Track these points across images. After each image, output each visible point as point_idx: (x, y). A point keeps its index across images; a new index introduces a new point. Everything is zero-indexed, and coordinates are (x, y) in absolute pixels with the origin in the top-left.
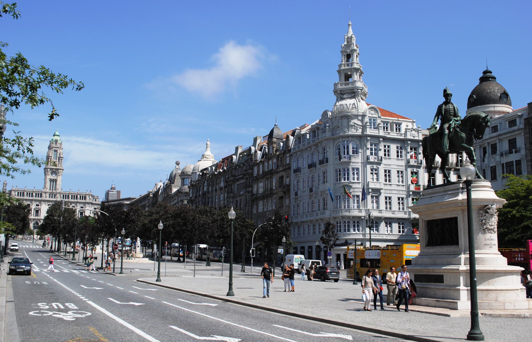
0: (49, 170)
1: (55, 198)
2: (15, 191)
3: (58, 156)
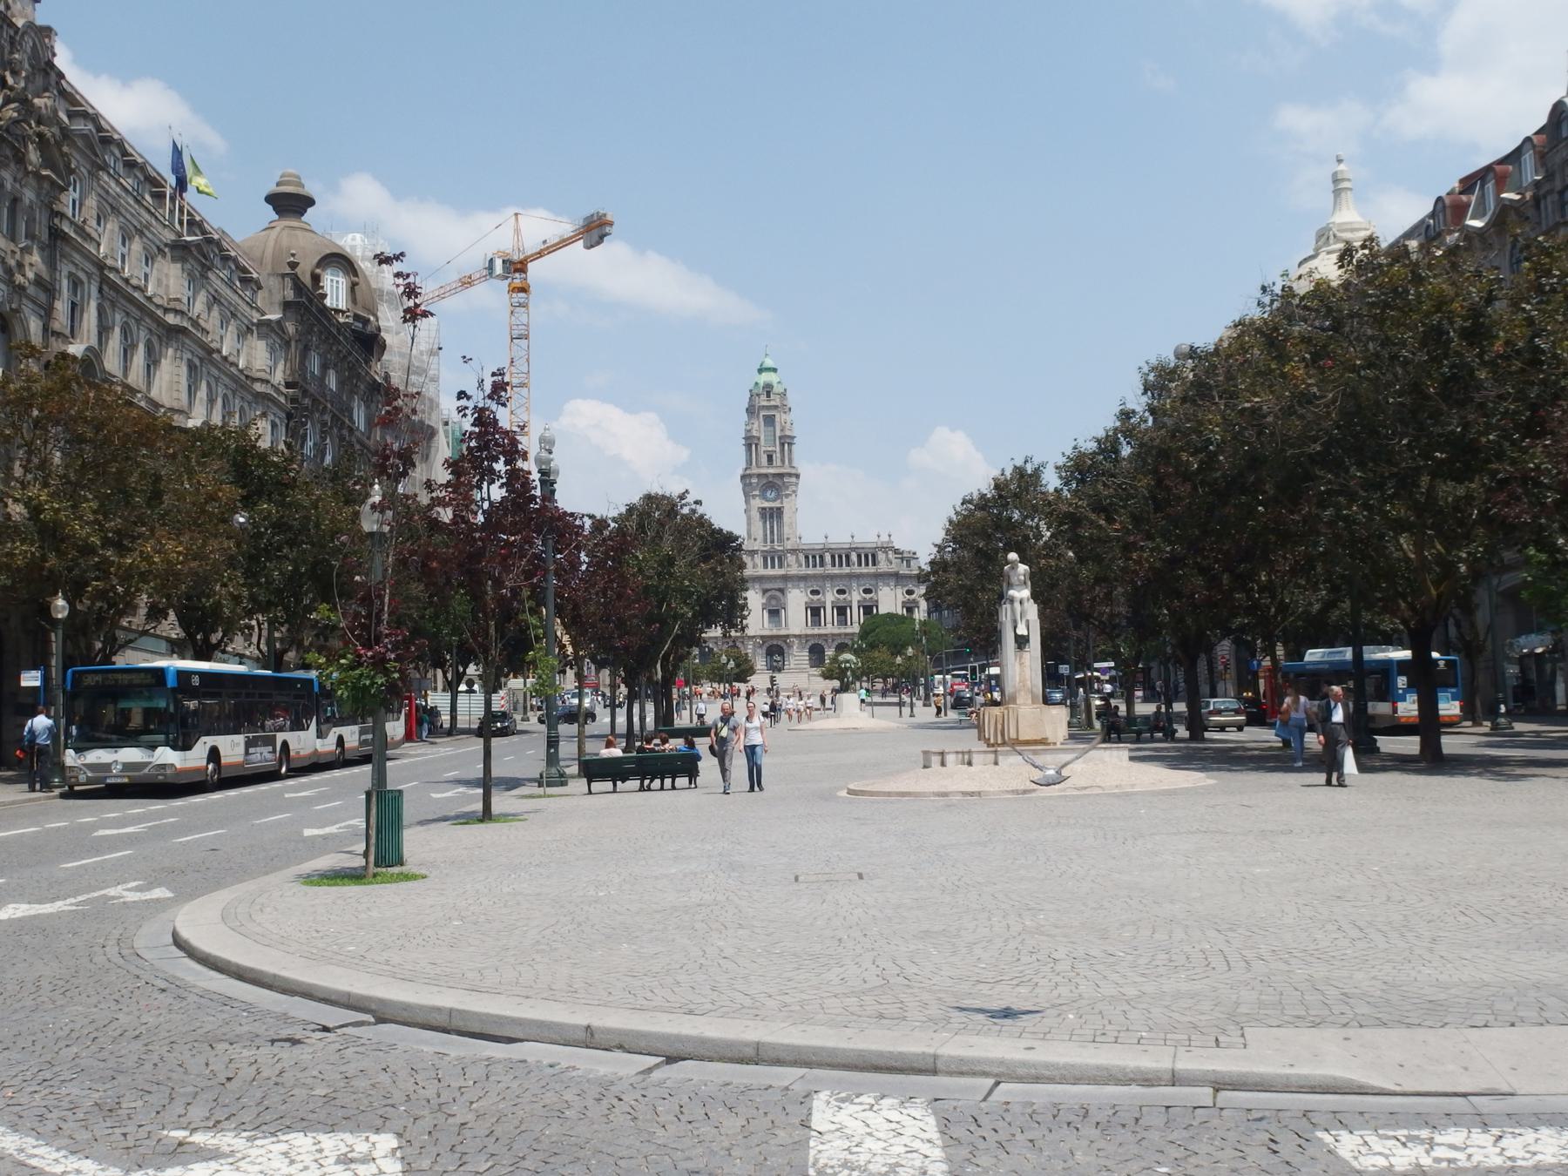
0: (754, 480)
1: (781, 566)
3: (778, 434)
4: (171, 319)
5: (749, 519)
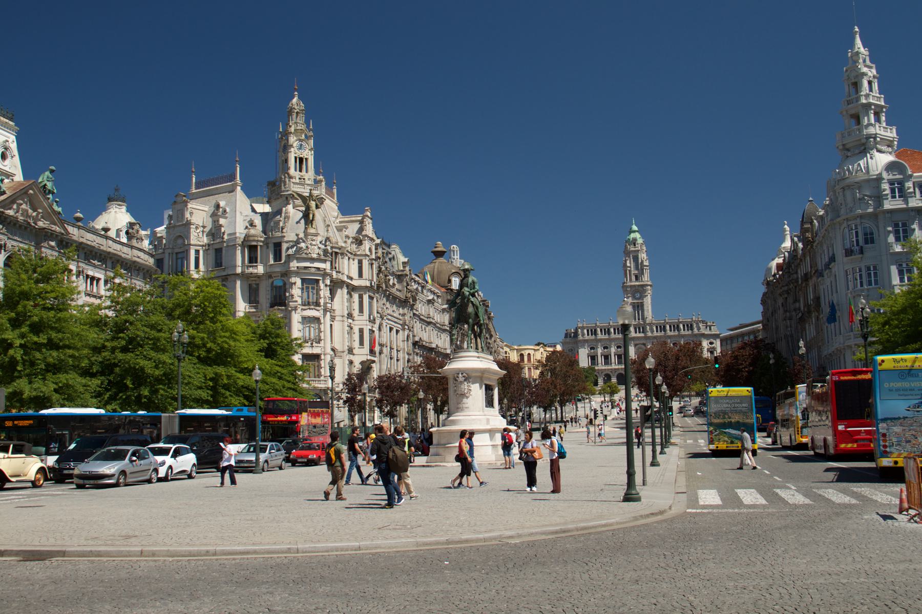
2: (583, 328)
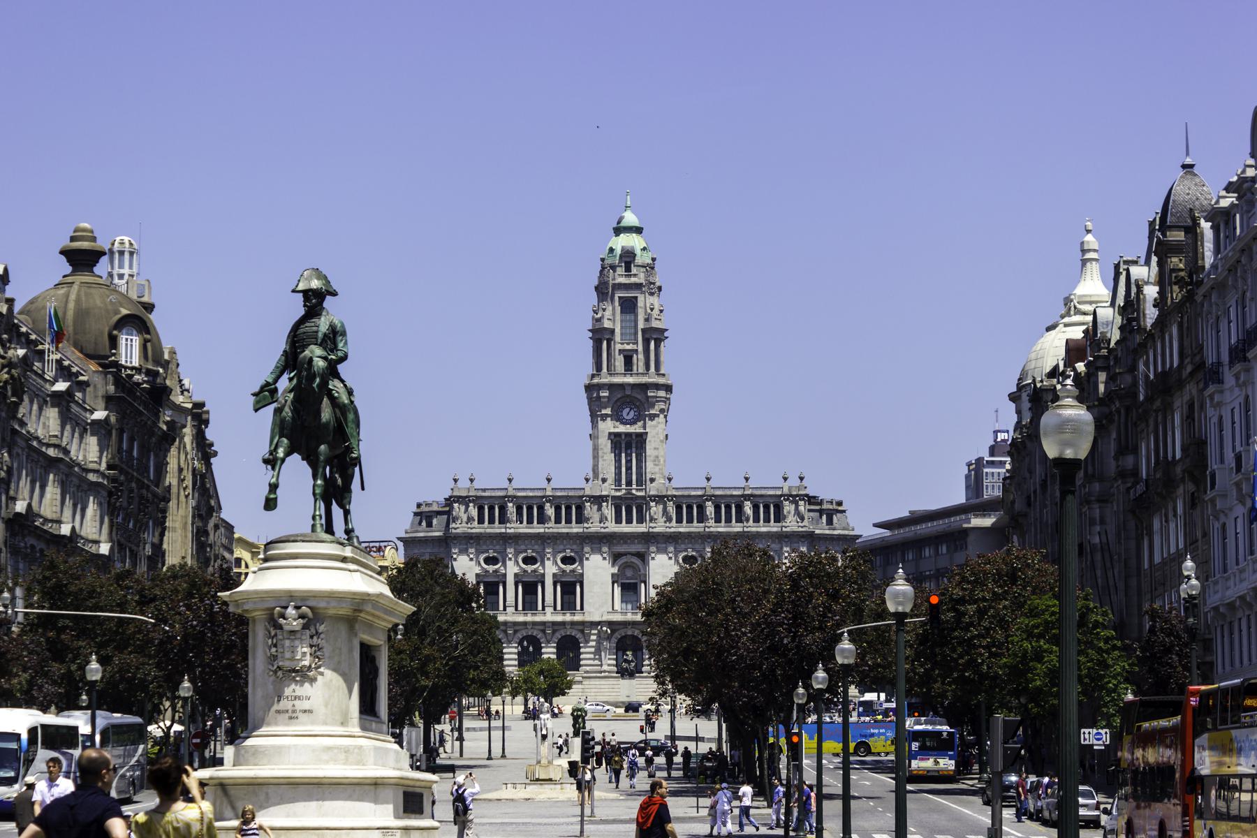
1: (641, 520)
2: (464, 500)
4: (51, 452)
5: (596, 449)
